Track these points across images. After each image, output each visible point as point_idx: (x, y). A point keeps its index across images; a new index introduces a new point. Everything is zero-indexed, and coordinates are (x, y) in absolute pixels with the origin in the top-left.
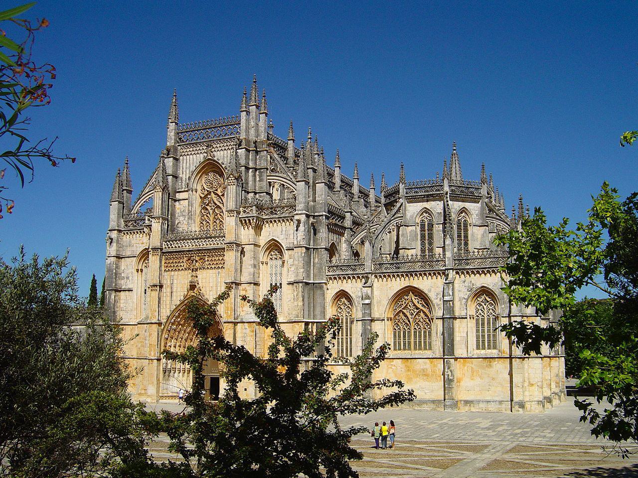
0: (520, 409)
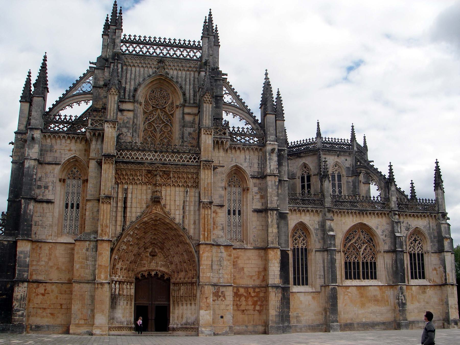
0: (455, 326)
